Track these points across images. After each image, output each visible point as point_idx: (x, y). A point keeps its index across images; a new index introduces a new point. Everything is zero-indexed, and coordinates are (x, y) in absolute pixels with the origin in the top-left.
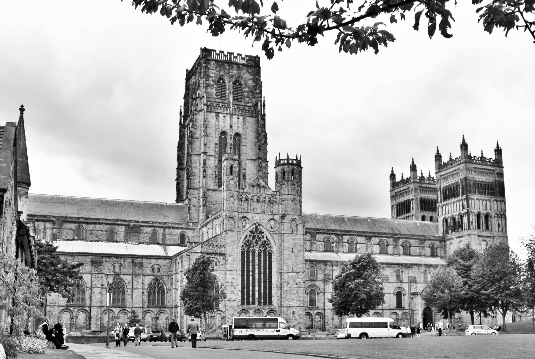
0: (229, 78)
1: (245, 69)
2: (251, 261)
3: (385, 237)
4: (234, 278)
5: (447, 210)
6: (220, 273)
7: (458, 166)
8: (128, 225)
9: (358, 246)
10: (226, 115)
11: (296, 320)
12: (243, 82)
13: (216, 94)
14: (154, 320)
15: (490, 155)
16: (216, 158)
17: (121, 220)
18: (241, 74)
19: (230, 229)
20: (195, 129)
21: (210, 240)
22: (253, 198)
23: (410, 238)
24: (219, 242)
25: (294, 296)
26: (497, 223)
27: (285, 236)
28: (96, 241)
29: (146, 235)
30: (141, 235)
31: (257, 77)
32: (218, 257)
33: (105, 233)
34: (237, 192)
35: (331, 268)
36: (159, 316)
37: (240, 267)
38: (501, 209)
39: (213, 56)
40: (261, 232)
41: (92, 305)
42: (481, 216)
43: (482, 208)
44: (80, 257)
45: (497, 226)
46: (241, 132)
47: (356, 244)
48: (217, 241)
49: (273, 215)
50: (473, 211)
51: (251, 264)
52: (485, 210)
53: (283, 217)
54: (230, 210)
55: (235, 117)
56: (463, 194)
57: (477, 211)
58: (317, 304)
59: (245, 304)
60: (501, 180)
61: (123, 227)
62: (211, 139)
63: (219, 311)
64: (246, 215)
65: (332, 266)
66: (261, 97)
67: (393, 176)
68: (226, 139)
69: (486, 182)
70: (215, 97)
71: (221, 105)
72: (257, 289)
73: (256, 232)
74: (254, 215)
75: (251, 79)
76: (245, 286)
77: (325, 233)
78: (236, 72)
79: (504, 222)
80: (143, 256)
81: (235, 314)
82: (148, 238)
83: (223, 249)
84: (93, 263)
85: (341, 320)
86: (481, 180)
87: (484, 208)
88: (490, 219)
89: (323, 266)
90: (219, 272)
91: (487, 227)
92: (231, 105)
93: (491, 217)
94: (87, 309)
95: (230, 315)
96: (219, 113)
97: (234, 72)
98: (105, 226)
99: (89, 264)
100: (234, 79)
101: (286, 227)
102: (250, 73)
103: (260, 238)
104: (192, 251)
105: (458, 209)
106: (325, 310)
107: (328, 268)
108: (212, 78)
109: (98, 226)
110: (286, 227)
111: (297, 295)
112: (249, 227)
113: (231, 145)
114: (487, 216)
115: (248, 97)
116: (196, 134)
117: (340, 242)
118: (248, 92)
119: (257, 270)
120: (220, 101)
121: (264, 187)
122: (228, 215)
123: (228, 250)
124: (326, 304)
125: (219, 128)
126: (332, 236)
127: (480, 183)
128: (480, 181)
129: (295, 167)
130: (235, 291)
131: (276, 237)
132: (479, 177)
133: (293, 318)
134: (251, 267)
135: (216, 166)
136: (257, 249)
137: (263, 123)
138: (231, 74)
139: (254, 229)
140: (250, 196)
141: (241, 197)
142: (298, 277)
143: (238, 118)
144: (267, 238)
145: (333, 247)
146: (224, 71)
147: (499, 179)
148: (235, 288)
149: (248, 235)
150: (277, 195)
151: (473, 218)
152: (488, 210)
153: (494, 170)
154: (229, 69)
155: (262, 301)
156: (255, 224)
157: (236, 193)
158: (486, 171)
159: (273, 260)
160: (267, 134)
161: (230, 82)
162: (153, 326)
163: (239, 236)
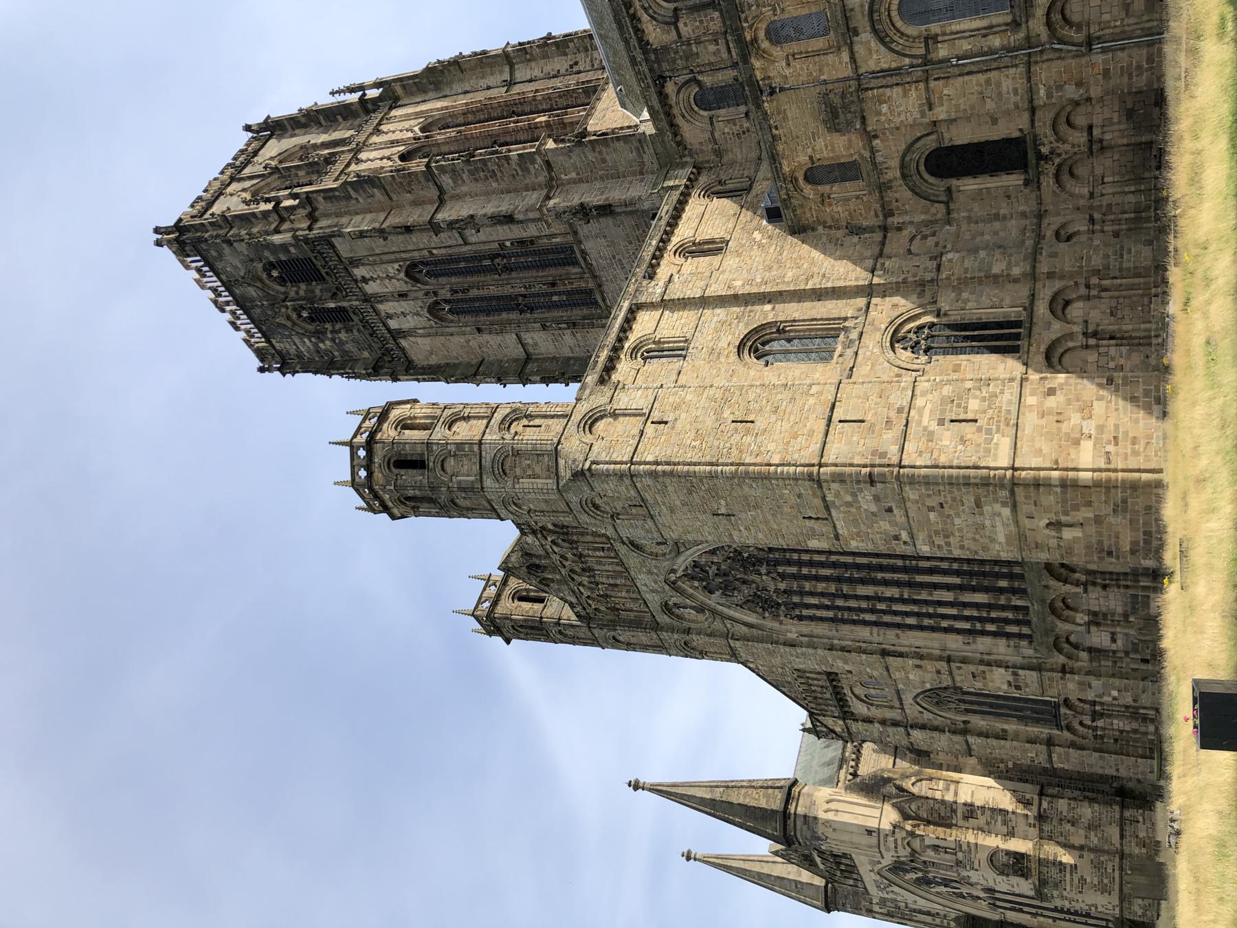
10: (383, 314)
11: (1098, 520)
25: (957, 521)
40: (696, 565)
55: (371, 288)
72: (948, 596)
90: (901, 686)
111: (947, 510)
133: (1092, 530)
139: (696, 584)
142: (849, 504)
144: (713, 552)
155: (1003, 583)
156: (673, 585)
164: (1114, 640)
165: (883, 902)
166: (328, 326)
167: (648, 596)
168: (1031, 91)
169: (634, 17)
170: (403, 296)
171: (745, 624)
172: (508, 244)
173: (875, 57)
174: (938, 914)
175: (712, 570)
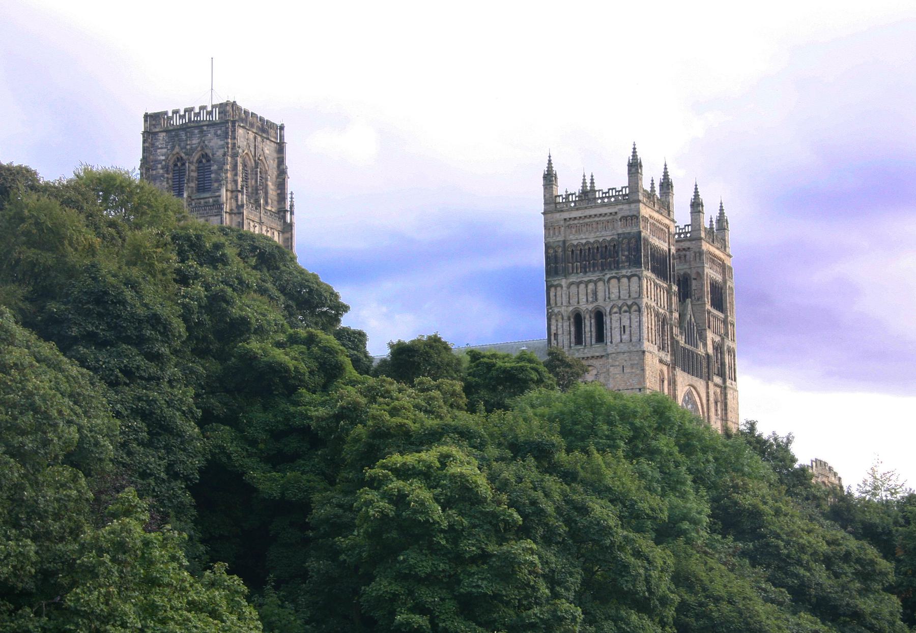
1: (212, 131)
18: (206, 142)
26: (618, 325)
43: (585, 300)
52: (592, 302)
57: (571, 308)
86: (584, 241)
87: (590, 299)
91: (600, 338)
97: (194, 142)
100: (196, 157)
108: (161, 163)
114: (599, 316)
137: (239, 220)
146: (179, 145)
147: (628, 230)
152: (600, 302)
153: (616, 213)
154: (187, 140)
158: (597, 219)
166: (170, 176)
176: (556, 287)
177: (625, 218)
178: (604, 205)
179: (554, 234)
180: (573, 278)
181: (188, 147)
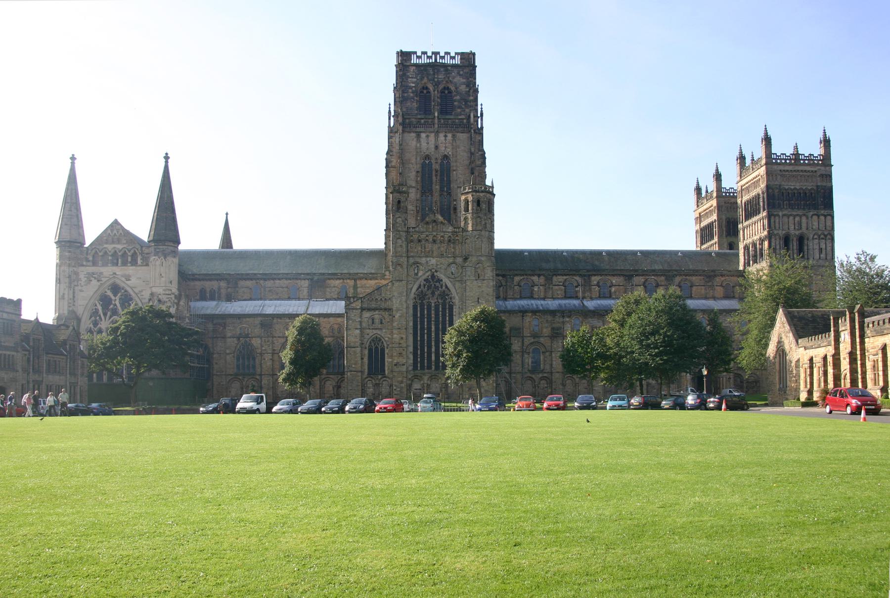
0: (434, 86)
1: (456, 71)
2: (426, 316)
3: (653, 275)
4: (402, 338)
5: (748, 233)
6: (385, 332)
7: (759, 170)
8: (312, 279)
9: (613, 289)
12: (453, 88)
13: (419, 109)
14: (336, 389)
15: (817, 150)
16: (418, 189)
17: (304, 274)
18: (450, 79)
19: (398, 279)
20: (391, 155)
21: (372, 294)
22: (427, 238)
23: (691, 275)
24: (383, 295)
26: (817, 247)
27: (468, 283)
28: (276, 299)
29: (333, 289)
30: (328, 290)
31: (470, 79)
32: (384, 313)
33: (286, 289)
34: (406, 232)
35: (561, 319)
36: (342, 384)
37: (411, 324)
38: (825, 226)
39: (414, 60)
40: (440, 281)
41: (263, 373)
42: (791, 239)
43: (793, 227)
44: (248, 319)
45: (817, 252)
46: (450, 153)
47: (610, 287)
48: (381, 294)
49: (454, 257)
50: (776, 232)
51: (426, 320)
52: (798, 230)
53: (466, 259)
54: (398, 255)
55: (441, 136)
56: (764, 210)
57: (784, 232)
58: (542, 366)
59: (419, 368)
60: (828, 185)
61: (307, 281)
62: (411, 166)
63: (385, 377)
64: (418, 260)
65: (563, 317)
66: (477, 105)
67: (698, 190)
68: (430, 164)
69: (801, 189)
70: (416, 112)
71: (422, 121)
72: (433, 350)
73: (433, 280)
74: (428, 259)
75: (464, 84)
76: (419, 347)
77: (566, 275)
78: (443, 77)
79: (829, 245)
80: (319, 314)
81: (405, 380)
82: (336, 293)
83: (389, 303)
84: (262, 325)
85: (576, 386)
86: (792, 187)
87: (797, 228)
88: (806, 242)
89: (550, 318)
90: (384, 331)
92: (436, 121)
93: (808, 239)
94: (258, 377)
95: (398, 382)
96: (421, 132)
97: (440, 77)
98: (285, 282)
99: (259, 326)
100: (441, 87)
101: (470, 272)
102: (462, 75)
103: (437, 288)
104: (350, 307)
105: (759, 231)
106: (552, 373)
107: (557, 320)
108: (412, 89)
109: (277, 282)
110: (470, 272)
112: (423, 275)
113: (437, 171)
114: (801, 239)
115: (459, 107)
116: (392, 161)
117: (587, 284)
118: (459, 101)
119: (433, 327)
120: (423, 116)
121: (442, 222)
122: (394, 261)
123: (396, 304)
124: (553, 366)
125: (421, 152)
126: (575, 278)
127: (790, 192)
128: (791, 189)
129: (482, 194)
130: (404, 353)
131: (458, 285)
132: (790, 183)
134: (426, 324)
135: (417, 200)
136: (433, 303)
138: (436, 80)
140: (423, 236)
141: (412, 238)
143: (446, 136)
144: (446, 287)
145: (577, 292)
146: (428, 77)
147: (824, 184)
148: (404, 350)
149: (422, 284)
150: (459, 232)
151: (777, 243)
153: (816, 171)
154: (434, 74)
157: (404, 234)
158: (801, 173)
159: (454, 314)
160: (485, 153)
161: (434, 91)
162: (335, 395)
163: (410, 287)
164: (416, 389)
165: (76, 274)
166: (418, 99)
167: (424, 259)
168: (515, 373)
169: (523, 275)
170: (437, 147)
171: (412, 288)
172: (455, 203)
173: (527, 341)
174: (74, 301)
175: (437, 284)
176: (775, 216)
177: (822, 176)
178: (804, 164)
179: (773, 179)
180: (785, 212)
181: (436, 80)
